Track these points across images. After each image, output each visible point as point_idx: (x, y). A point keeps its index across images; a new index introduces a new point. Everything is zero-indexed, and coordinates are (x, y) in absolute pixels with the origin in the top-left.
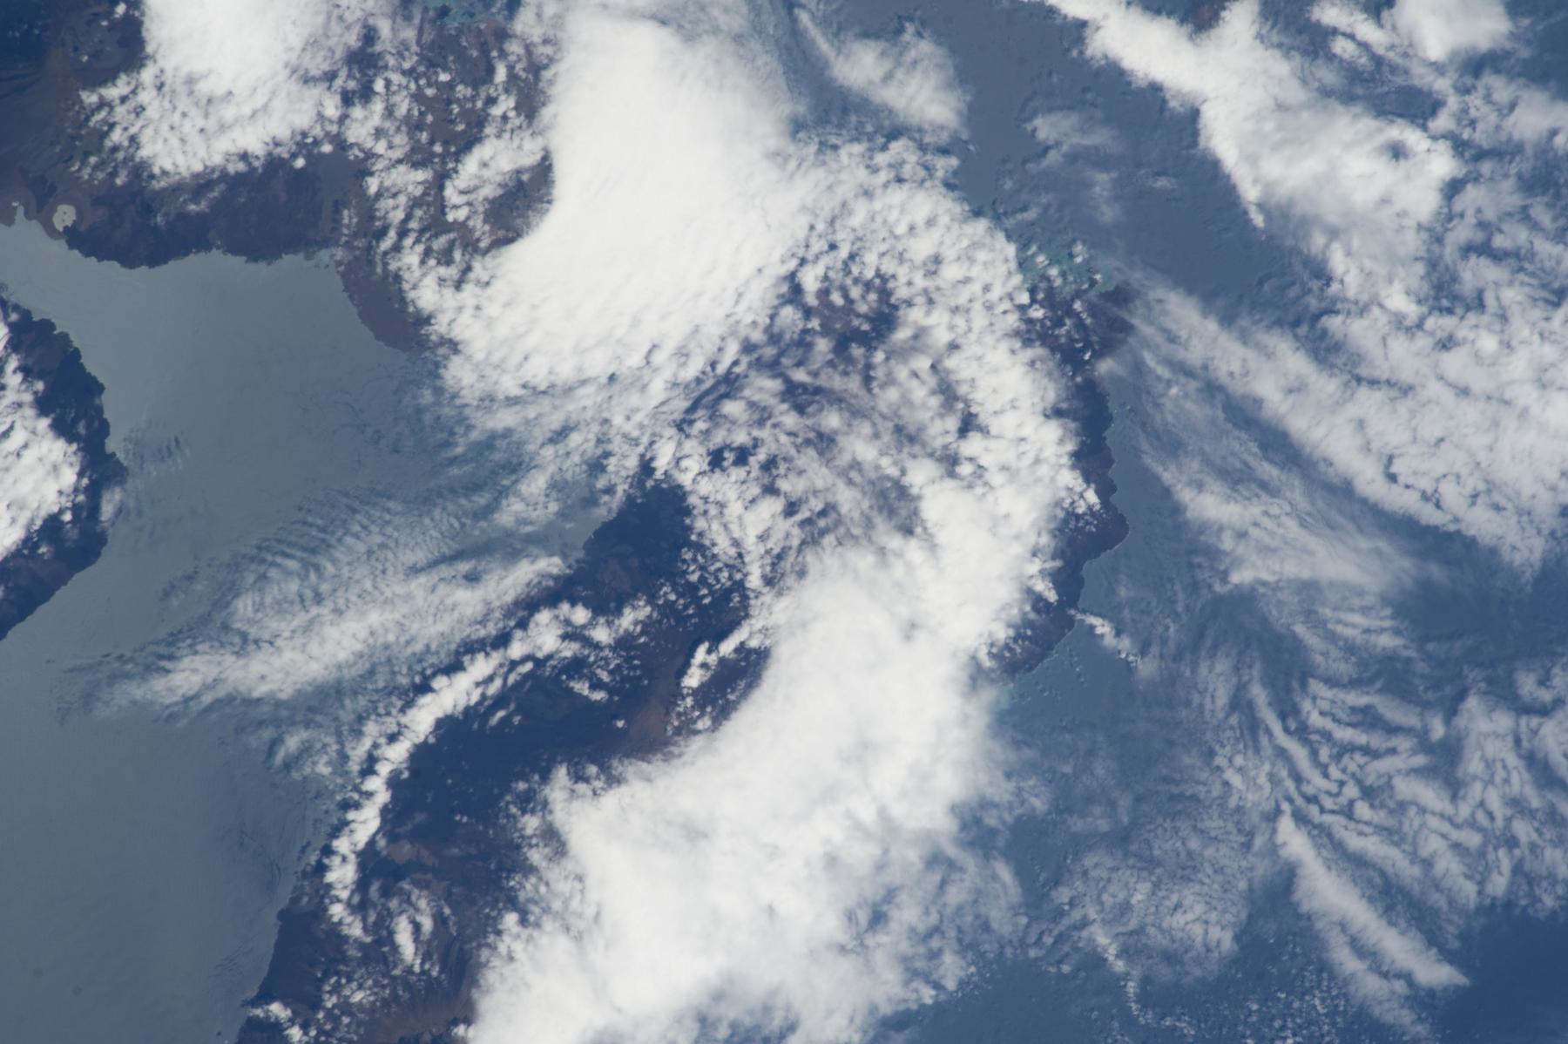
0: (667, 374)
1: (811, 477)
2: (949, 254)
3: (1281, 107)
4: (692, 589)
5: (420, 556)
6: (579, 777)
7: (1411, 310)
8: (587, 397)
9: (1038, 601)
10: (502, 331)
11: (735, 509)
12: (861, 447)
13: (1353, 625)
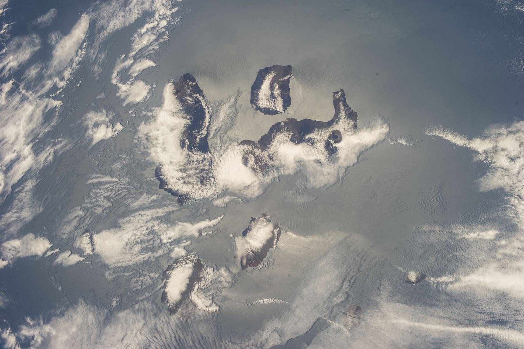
1: (194, 165)
3: (185, 232)
4: (195, 147)
5: (222, 127)
7: (154, 228)
8: (222, 152)
9: (162, 175)
11: (198, 157)
12: (193, 172)
13: (130, 200)
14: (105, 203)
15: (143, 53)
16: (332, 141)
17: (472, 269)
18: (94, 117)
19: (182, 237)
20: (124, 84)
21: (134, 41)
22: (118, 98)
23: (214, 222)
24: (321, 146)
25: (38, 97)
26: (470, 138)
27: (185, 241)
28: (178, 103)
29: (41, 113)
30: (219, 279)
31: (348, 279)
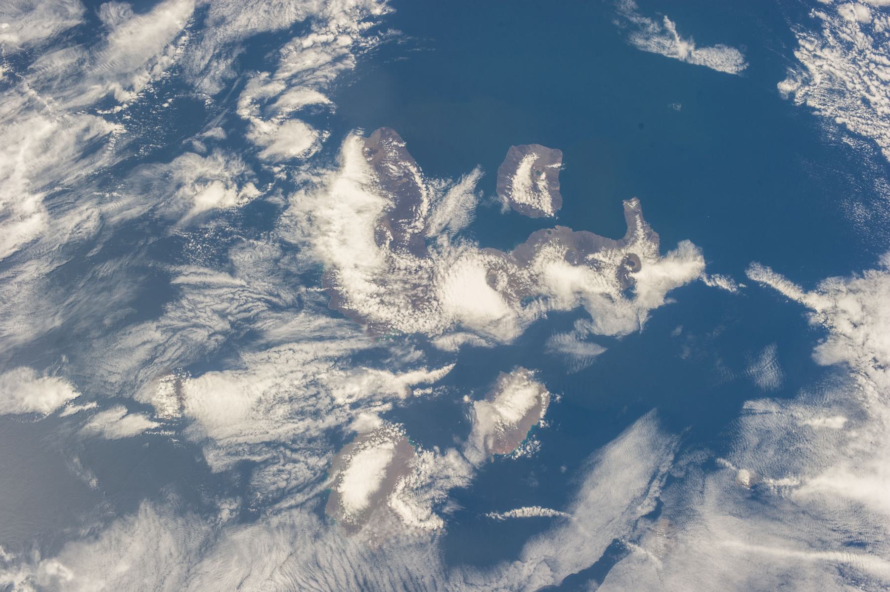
0: (442, 273)
2: (415, 325)
4: (403, 246)
5: (452, 222)
6: (390, 208)
7: (319, 377)
8: (451, 261)
9: (337, 285)
10: (475, 260)
11: (409, 263)
12: (398, 286)
13: (269, 323)
14: (215, 323)
15: (305, 78)
16: (629, 268)
17: (820, 466)
18: (198, 165)
19: (374, 395)
20: (262, 120)
21: (287, 55)
22: (251, 144)
23: (436, 374)
25: (69, 110)
26: (806, 292)
27: (380, 403)
29: (73, 140)
30: (446, 472)
31: (658, 477)
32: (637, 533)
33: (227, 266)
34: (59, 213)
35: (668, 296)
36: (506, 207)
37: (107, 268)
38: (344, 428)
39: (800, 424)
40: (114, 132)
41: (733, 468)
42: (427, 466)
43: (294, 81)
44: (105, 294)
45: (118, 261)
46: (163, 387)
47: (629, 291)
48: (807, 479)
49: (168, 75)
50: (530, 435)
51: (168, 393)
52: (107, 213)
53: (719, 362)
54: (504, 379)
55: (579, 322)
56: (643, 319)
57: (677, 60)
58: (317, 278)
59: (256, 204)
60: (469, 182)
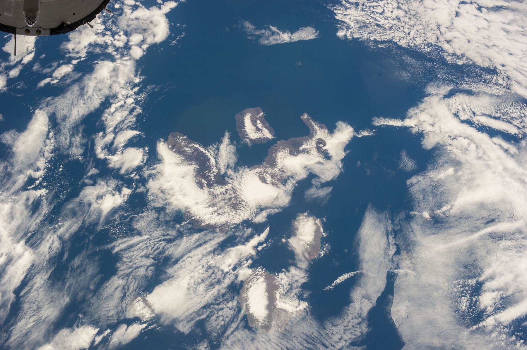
4: (213, 184)
5: (229, 162)
7: (209, 264)
8: (239, 180)
9: (193, 216)
15: (121, 127)
18: (93, 191)
19: (240, 259)
20: (112, 155)
21: (106, 120)
22: (113, 169)
24: (314, 152)
26: (403, 120)
28: (178, 155)
32: (395, 264)
33: (135, 232)
34: (37, 246)
35: (345, 150)
36: (249, 143)
37: (77, 261)
38: (236, 282)
39: (435, 180)
40: (42, 194)
41: (419, 214)
42: (285, 280)
43: (117, 130)
44: (83, 274)
45: (80, 255)
46: (138, 305)
47: (327, 156)
48: (453, 203)
49: (53, 155)
50: (322, 243)
51: (142, 307)
52: (61, 235)
53: (385, 169)
54: (296, 223)
55: (313, 180)
56: (341, 166)
57: (286, 43)
58: (182, 217)
59: (132, 198)
60: (226, 140)
